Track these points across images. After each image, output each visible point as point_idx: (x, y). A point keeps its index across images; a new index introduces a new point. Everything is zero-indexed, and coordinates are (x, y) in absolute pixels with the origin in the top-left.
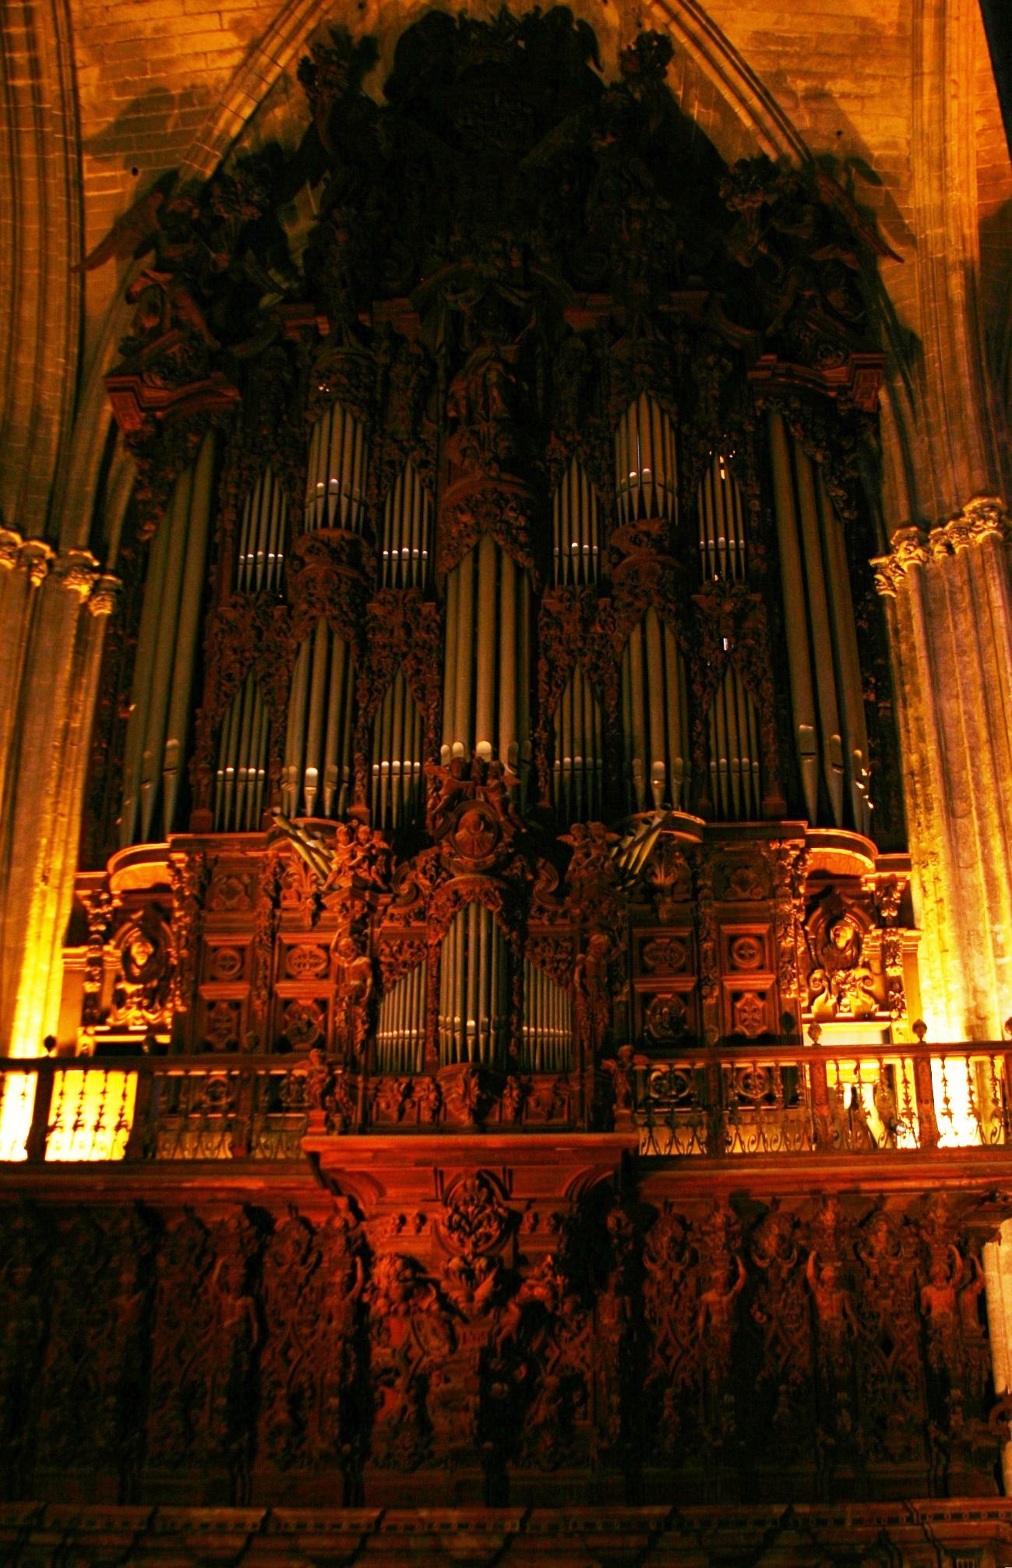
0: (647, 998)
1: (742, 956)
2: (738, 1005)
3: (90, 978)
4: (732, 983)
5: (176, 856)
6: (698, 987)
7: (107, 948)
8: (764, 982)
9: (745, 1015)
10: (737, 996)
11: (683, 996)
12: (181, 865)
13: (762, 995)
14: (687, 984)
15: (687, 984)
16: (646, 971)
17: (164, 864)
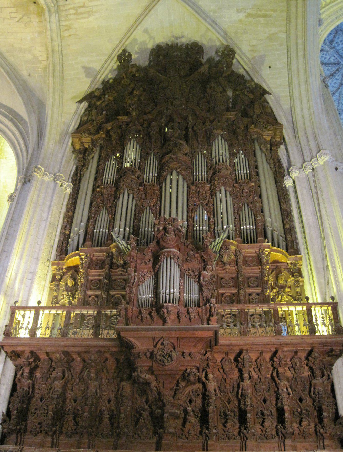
0: (223, 295)
1: (251, 283)
2: (251, 297)
3: (56, 291)
4: (249, 291)
5: (81, 254)
6: (238, 291)
7: (60, 282)
8: (258, 290)
9: (253, 300)
10: (250, 294)
11: (234, 294)
12: (83, 257)
13: (258, 294)
14: (234, 291)
15: (234, 291)
16: (223, 287)
17: (78, 257)
